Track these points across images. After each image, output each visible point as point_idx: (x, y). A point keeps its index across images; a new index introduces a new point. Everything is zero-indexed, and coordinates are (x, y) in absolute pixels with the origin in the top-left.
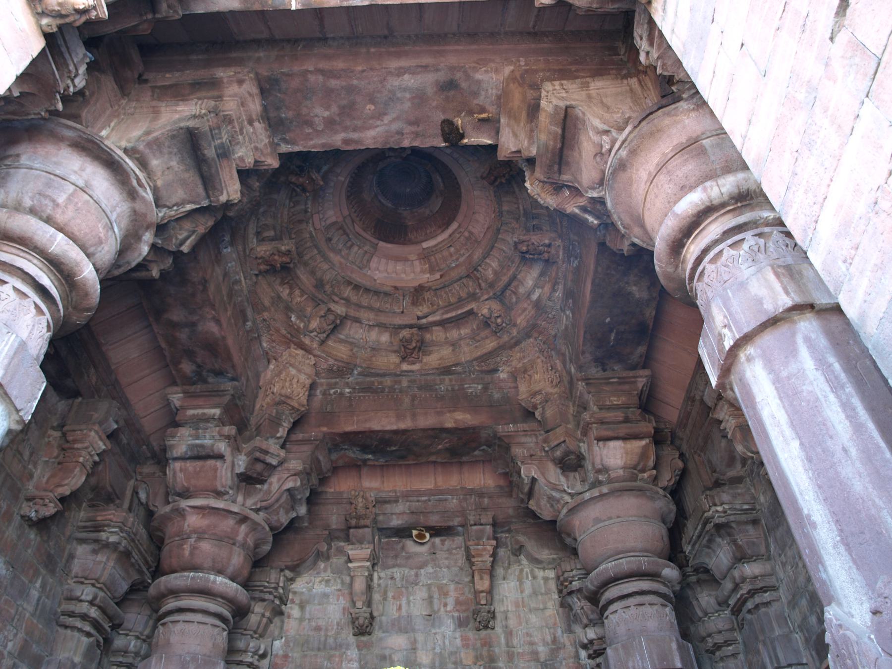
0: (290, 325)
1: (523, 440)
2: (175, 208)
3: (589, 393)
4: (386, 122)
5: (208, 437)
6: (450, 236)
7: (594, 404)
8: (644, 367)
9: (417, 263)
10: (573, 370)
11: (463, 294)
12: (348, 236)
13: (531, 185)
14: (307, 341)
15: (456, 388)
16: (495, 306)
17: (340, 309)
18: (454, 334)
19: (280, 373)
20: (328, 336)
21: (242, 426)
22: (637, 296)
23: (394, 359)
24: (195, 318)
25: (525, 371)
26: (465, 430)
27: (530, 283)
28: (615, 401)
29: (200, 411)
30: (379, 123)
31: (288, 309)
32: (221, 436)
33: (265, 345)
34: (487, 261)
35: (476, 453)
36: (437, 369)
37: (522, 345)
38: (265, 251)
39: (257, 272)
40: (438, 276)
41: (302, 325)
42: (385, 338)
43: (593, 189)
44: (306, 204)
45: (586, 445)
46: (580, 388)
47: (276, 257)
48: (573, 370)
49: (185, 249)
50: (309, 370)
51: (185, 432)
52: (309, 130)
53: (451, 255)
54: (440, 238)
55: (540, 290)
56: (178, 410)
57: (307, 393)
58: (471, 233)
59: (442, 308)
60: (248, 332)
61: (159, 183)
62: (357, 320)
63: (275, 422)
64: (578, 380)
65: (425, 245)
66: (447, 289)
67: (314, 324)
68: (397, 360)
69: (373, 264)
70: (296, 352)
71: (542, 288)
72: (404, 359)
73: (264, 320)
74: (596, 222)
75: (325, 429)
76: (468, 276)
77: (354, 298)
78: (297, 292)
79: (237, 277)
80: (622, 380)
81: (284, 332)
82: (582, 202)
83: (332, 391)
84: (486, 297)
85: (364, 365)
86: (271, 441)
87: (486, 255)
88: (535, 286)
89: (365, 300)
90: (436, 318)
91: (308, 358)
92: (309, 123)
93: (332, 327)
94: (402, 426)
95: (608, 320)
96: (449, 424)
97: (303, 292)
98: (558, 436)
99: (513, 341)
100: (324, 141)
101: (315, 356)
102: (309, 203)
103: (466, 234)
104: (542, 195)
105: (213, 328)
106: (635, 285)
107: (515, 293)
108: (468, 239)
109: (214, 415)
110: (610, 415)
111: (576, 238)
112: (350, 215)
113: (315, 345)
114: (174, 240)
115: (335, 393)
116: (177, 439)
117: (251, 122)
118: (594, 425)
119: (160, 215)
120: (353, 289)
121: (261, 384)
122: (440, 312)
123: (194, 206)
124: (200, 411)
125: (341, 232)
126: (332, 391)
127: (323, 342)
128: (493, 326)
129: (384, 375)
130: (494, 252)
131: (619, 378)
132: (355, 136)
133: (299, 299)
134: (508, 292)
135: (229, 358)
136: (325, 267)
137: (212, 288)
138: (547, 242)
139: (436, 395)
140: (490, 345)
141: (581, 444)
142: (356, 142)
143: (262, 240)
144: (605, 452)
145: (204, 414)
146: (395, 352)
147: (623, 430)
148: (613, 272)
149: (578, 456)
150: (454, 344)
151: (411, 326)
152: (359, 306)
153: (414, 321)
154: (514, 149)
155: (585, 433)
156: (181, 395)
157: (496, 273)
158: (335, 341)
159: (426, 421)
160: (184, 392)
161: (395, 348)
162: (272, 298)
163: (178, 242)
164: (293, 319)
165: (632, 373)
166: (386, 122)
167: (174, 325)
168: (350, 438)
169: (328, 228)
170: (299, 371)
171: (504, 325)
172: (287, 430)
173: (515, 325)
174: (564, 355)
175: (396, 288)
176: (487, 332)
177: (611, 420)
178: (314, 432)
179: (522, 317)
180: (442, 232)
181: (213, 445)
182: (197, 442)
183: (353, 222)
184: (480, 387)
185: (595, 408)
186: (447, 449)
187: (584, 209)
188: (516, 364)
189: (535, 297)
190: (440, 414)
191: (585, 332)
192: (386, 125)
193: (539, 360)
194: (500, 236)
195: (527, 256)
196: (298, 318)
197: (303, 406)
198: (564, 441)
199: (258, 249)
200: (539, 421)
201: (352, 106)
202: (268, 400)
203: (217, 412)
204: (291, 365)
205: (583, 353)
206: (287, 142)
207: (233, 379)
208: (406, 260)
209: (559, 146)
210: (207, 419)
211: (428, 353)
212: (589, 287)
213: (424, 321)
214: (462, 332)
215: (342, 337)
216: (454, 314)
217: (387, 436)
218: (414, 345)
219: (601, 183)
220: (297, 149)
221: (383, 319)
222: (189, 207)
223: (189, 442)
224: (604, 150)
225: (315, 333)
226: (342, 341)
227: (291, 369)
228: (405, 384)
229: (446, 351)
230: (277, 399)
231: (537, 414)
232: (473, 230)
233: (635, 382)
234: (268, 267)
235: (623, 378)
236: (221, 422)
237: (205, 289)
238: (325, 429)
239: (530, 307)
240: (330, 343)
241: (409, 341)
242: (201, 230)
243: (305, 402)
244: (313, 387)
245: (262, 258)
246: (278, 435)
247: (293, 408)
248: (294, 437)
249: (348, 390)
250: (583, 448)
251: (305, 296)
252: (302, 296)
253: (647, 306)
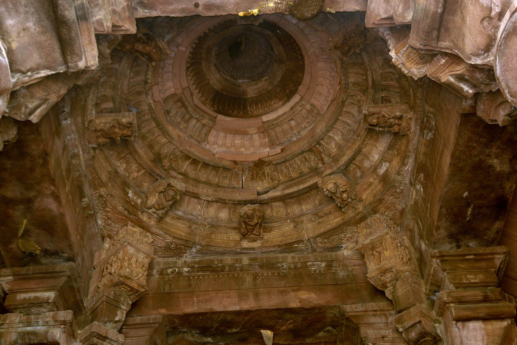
0: (127, 202)
1: (372, 320)
2: (29, 74)
3: (444, 270)
5: (41, 323)
6: (292, 109)
7: (451, 283)
8: (500, 244)
9: (256, 137)
10: (423, 246)
11: (305, 170)
12: (186, 108)
13: (396, 54)
14: (145, 218)
15: (299, 265)
16: (341, 180)
17: (179, 185)
18: (295, 209)
19: (117, 252)
20: (167, 212)
21: (77, 308)
22: (498, 169)
23: (235, 236)
24: (32, 194)
25: (373, 249)
26: (313, 309)
27: (376, 157)
28: (472, 278)
29: (32, 295)
31: (125, 185)
32: (56, 321)
33: (100, 222)
35: (321, 334)
36: (279, 246)
37: (368, 221)
38: (105, 123)
39: (95, 146)
40: (278, 150)
41: (139, 201)
42: (224, 214)
43: (478, 55)
44: (147, 74)
45: (442, 326)
46: (435, 265)
47: (117, 130)
48: (423, 246)
49: (34, 118)
50: (146, 248)
51: (15, 318)
53: (292, 128)
54: (280, 112)
55: (388, 164)
56: (6, 294)
57: (146, 273)
58: (312, 105)
59: (283, 183)
60: (84, 209)
61: (14, 45)
62: (196, 196)
63: (113, 305)
64: (433, 257)
65: (265, 118)
66: (288, 164)
67: (153, 200)
68: (237, 237)
69: (211, 138)
70: (134, 229)
71: (390, 162)
72: (244, 236)
73: (101, 196)
74: (471, 91)
75: (163, 311)
76: (310, 150)
77: (192, 174)
78: (134, 167)
79: (76, 151)
80: (479, 257)
81: (120, 208)
82: (460, 69)
83: (170, 271)
84: (329, 171)
85: (203, 243)
86: (109, 325)
87: (330, 128)
88: (382, 160)
89: (203, 175)
90: (277, 193)
91: (146, 236)
93: (171, 203)
94: (245, 306)
95: (466, 194)
96: (294, 305)
97: (141, 166)
98: (413, 315)
99: (358, 217)
100: (184, 6)
101: (152, 233)
102: (150, 73)
103: (308, 107)
104: (407, 64)
105: (52, 205)
106: (496, 158)
107: (359, 168)
108: (309, 112)
109: (48, 298)
110: (469, 294)
111: (432, 110)
113: (152, 222)
114: (23, 109)
115: (172, 273)
116: (5, 326)
118: (452, 305)
119: (13, 80)
120: (191, 164)
121: (95, 263)
122: (281, 187)
123: (50, 73)
124: (32, 295)
125: (179, 104)
126: (170, 271)
127: (160, 219)
128: (338, 201)
129: (223, 253)
130: (338, 126)
131: (475, 255)
133: (136, 174)
134: (352, 167)
135: (66, 235)
136: (164, 140)
137: (52, 161)
138: (398, 114)
139: (278, 274)
140: (335, 220)
141: (437, 325)
143: (100, 113)
144: (465, 333)
145: (37, 298)
146: (235, 228)
147: (483, 309)
148: (474, 145)
149: (435, 338)
150: (296, 221)
151: (252, 202)
152: (197, 181)
153: (253, 197)
154: (384, 16)
155: (441, 314)
156: (11, 278)
157: (339, 147)
158: (173, 218)
159: (270, 302)
160: (14, 275)
161: (234, 225)
162: (109, 173)
163: (28, 110)
164: (130, 195)
165: (489, 250)
168: (190, 321)
169: (166, 100)
170: (138, 250)
171: (349, 200)
172: (125, 312)
173: (361, 200)
174: (411, 231)
175: (235, 162)
176: (331, 207)
177: (470, 299)
178: (155, 314)
179: (368, 192)
180: (283, 104)
181: (47, 332)
182: (28, 328)
183: (192, 94)
184: (323, 265)
185: (452, 287)
186: (290, 331)
187: (460, 78)
188: (364, 241)
189: (382, 171)
190: (283, 292)
191: (441, 207)
193: (388, 237)
194: (344, 109)
195: (377, 129)
196: (135, 193)
197: (143, 287)
198: (420, 322)
199: (97, 121)
200: (391, 301)
202: (105, 280)
203: (51, 295)
204: (129, 244)
205: (438, 228)
206: (144, 6)
207: (71, 259)
208: (245, 133)
209: (440, 11)
210: (40, 303)
211: (268, 230)
212: (447, 160)
213: (265, 196)
214: (304, 208)
215: (180, 213)
216: (295, 189)
217: (229, 318)
218: (256, 221)
219: (488, 49)
220: (154, 14)
221: (222, 194)
222: (43, 73)
223: (19, 330)
224: (493, 14)
225: (153, 210)
226: (179, 218)
227: (129, 247)
228: (246, 261)
229: (288, 228)
230: (116, 280)
231: (387, 293)
232: (316, 103)
233: (493, 259)
234: (108, 140)
235: (480, 255)
236: (55, 306)
237: (46, 162)
238: (163, 311)
239: (377, 181)
240: (168, 219)
241: (250, 217)
242: (53, 99)
243: (144, 283)
244: (151, 267)
245: (101, 130)
246: (117, 319)
247: (132, 289)
248: (131, 321)
249: (186, 269)
250: (440, 329)
251: (143, 171)
252: (138, 171)
253: (508, 179)
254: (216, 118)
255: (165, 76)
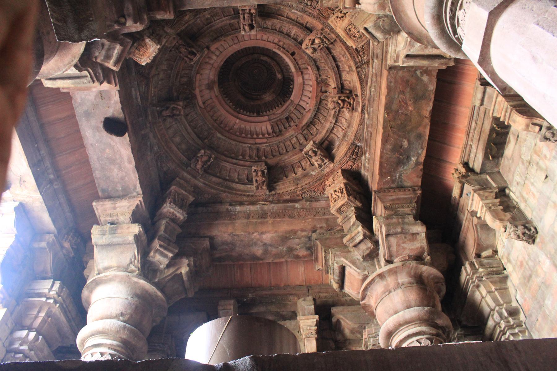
4: (114, 144)
14: (327, 170)
30: (115, 147)
34: (292, 34)
52: (126, 179)
92: (122, 178)
112: (268, 116)
117: (115, 208)
132: (126, 158)
142: (129, 158)
164: (314, 173)
166: (114, 144)
167: (266, 252)
175: (316, 97)
183: (274, 114)
192: (116, 144)
201: (108, 158)
206: (135, 188)
220: (138, 185)
254: (292, 101)
255: (258, 130)
